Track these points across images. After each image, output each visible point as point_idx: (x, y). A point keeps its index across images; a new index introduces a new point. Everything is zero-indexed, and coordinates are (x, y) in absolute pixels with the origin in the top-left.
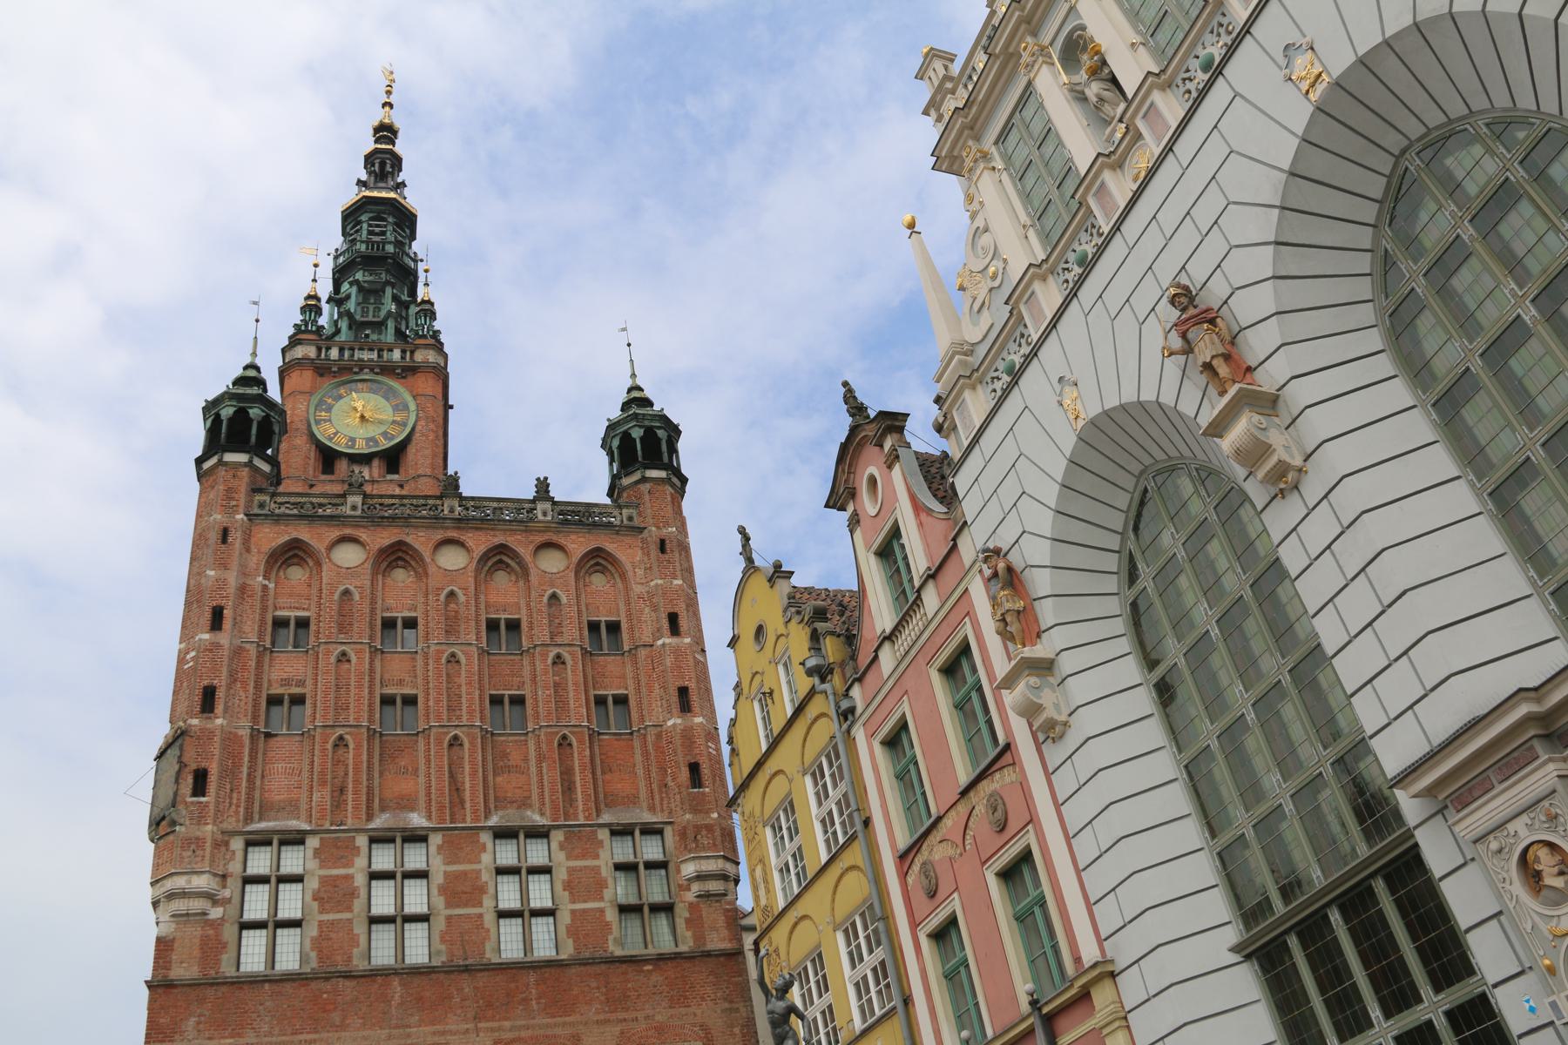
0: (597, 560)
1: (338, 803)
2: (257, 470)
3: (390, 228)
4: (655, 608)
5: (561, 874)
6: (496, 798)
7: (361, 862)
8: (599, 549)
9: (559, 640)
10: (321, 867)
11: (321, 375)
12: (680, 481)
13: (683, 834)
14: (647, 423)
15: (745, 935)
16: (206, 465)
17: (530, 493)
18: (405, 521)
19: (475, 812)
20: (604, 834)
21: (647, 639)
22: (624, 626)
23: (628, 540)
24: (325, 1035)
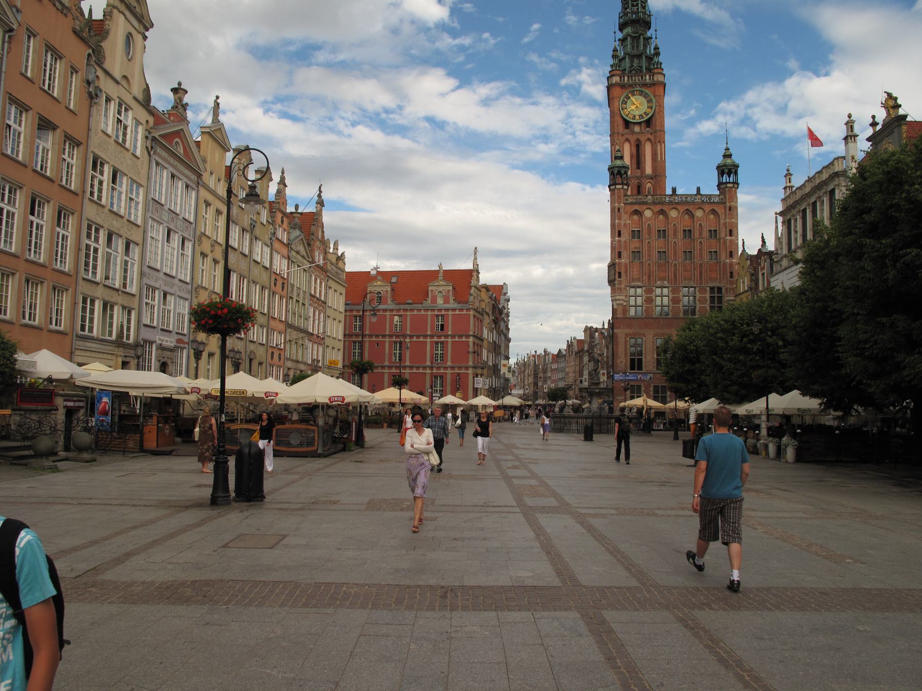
1: (649, 280)
13: (726, 289)
17: (695, 192)
20: (708, 289)
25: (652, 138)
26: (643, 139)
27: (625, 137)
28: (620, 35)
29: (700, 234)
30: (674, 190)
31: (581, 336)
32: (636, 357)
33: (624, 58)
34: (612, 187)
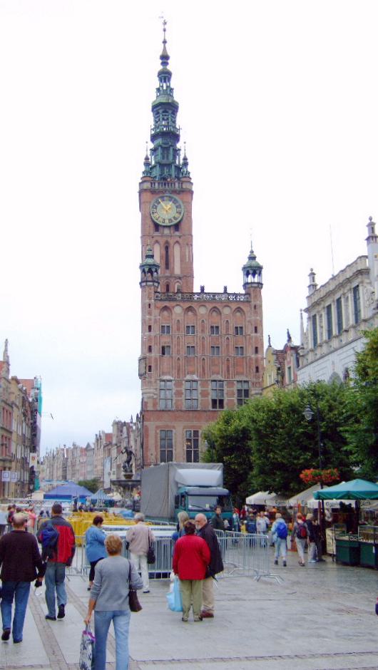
0: (239, 309)
5: (225, 392)
7: (184, 387)
11: (152, 194)
20: (235, 382)
21: (249, 333)
22: (244, 328)
23: (246, 304)
25: (181, 241)
26: (172, 241)
27: (154, 239)
28: (151, 146)
29: (227, 329)
30: (202, 289)
31: (109, 429)
33: (155, 166)
34: (144, 284)
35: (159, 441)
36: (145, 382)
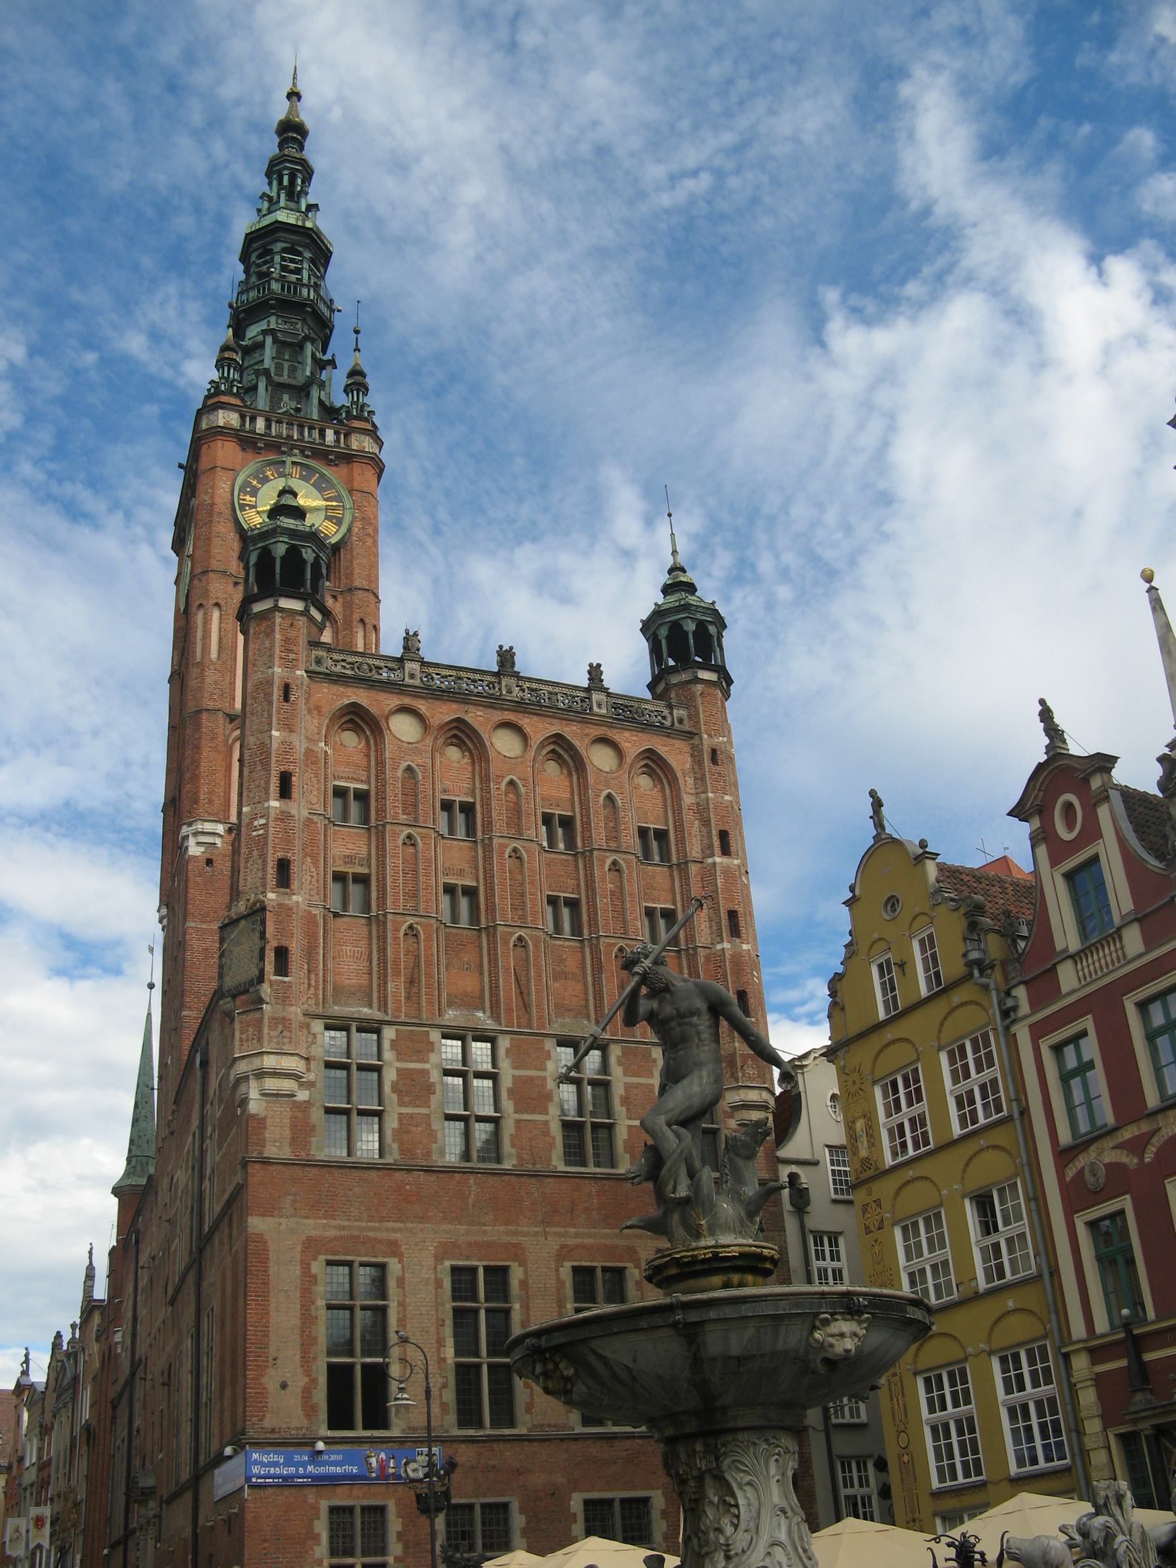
2: (312, 619)
3: (306, 265)
4: (706, 823)
5: (618, 1090)
6: (556, 1004)
7: (433, 1058)
8: (649, 750)
9: (613, 845)
10: (398, 1060)
12: (726, 679)
14: (699, 616)
15: (780, 1167)
16: (258, 607)
18: (462, 698)
19: (541, 1018)
23: (678, 744)
24: (410, 1225)
30: (506, 657)
32: (359, 1360)
35: (323, 1314)
36: (259, 1024)
